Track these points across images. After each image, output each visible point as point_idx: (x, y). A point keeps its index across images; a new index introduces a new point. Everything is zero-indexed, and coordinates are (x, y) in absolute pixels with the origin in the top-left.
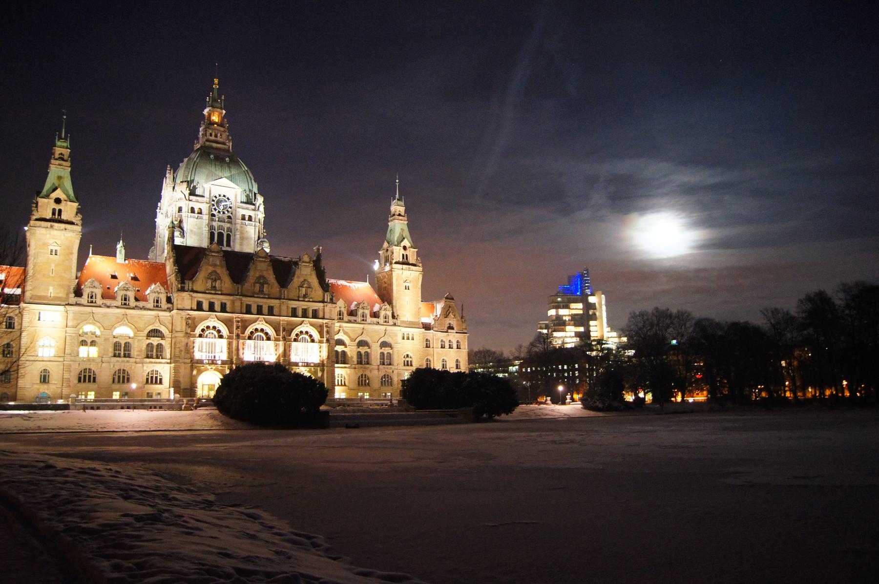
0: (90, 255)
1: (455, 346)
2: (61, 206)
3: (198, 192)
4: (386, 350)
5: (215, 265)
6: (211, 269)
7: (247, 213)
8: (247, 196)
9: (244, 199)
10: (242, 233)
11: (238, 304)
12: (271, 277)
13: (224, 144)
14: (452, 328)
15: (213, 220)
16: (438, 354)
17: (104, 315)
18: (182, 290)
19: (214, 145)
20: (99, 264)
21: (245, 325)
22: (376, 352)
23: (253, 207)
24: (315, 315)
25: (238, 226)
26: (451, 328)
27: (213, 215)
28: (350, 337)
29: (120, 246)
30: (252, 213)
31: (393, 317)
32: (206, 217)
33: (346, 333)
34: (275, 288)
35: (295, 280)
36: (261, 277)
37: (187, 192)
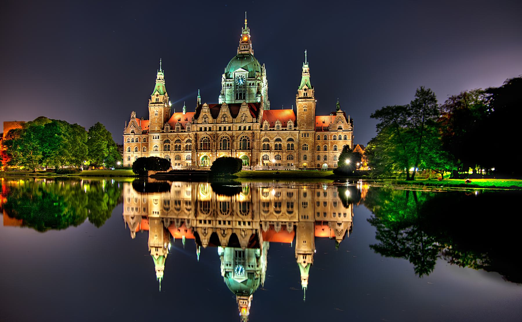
1: (343, 138)
2: (159, 97)
3: (231, 77)
6: (204, 114)
10: (249, 91)
11: (215, 127)
14: (342, 129)
15: (237, 88)
16: (331, 143)
18: (194, 123)
19: (243, 52)
22: (284, 144)
27: (237, 86)
29: (184, 109)
32: (233, 87)
34: (231, 119)
35: (239, 114)
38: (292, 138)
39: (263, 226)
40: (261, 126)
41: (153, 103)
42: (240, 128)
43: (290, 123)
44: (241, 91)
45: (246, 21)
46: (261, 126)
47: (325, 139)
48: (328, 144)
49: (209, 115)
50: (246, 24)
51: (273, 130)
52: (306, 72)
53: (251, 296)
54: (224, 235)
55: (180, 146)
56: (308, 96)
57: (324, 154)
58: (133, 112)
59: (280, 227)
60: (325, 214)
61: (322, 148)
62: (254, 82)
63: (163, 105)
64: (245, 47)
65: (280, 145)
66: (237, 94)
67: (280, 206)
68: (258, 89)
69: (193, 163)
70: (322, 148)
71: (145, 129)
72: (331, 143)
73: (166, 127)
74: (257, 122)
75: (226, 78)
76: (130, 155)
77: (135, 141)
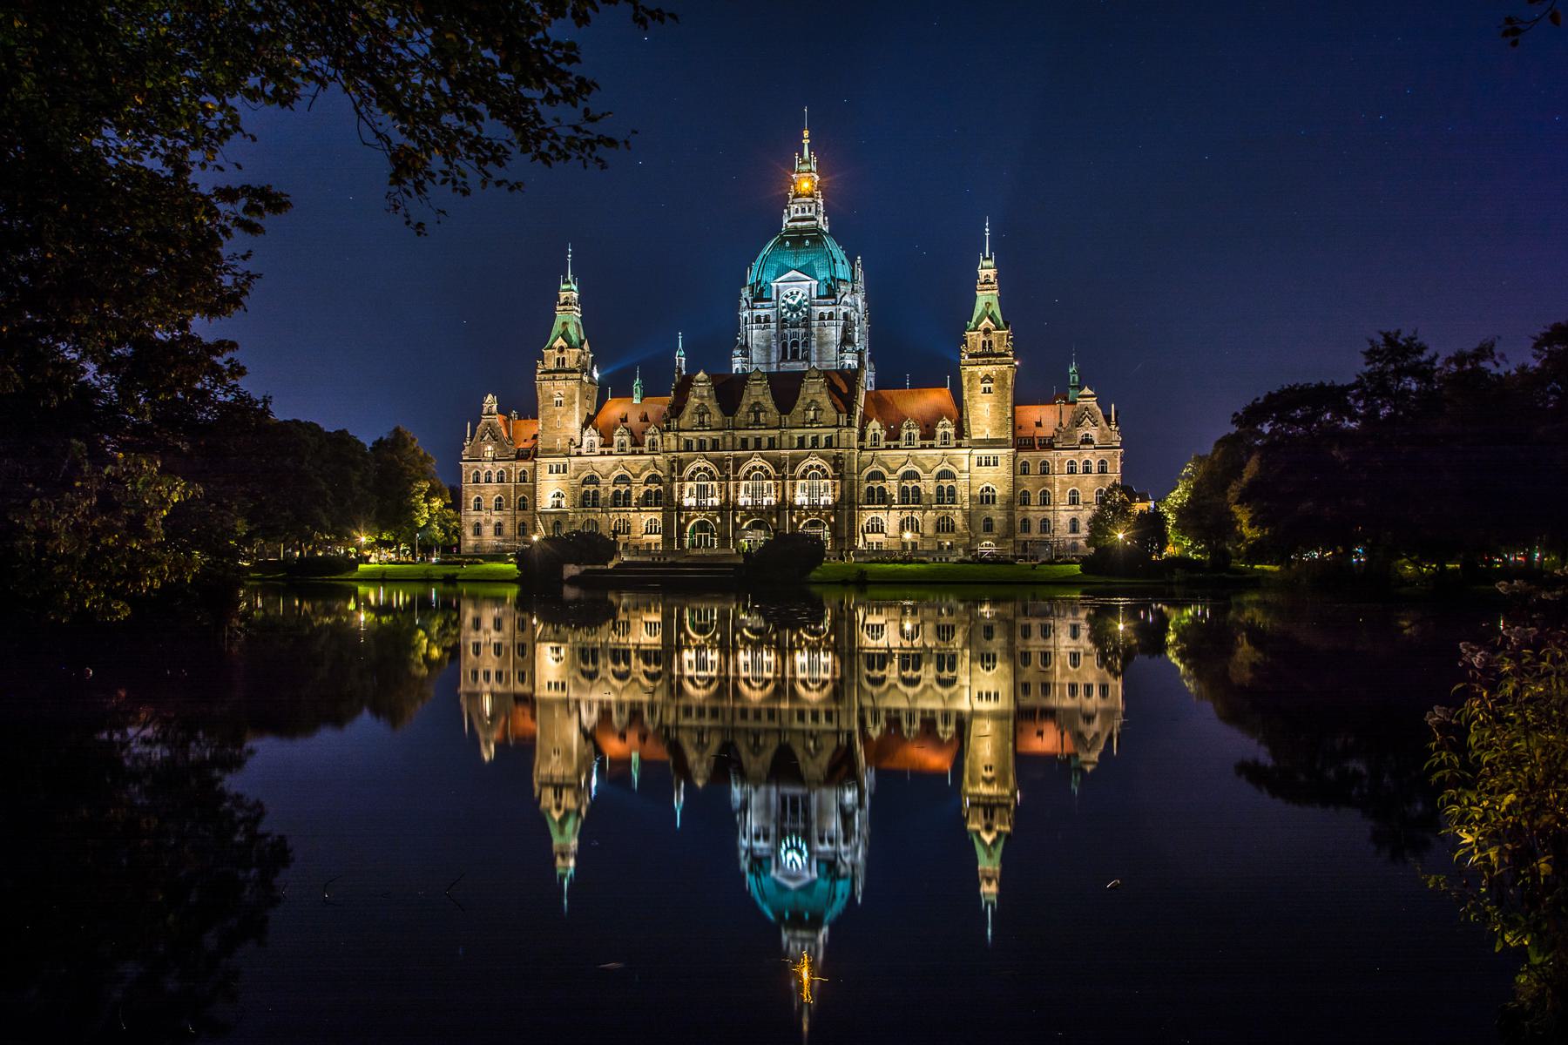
1: (1095, 468)
4: (946, 483)
5: (702, 397)
7: (826, 310)
8: (829, 287)
9: (823, 292)
10: (820, 338)
11: (729, 439)
12: (769, 403)
13: (813, 219)
16: (1062, 482)
17: (602, 464)
18: (668, 429)
20: (615, 409)
21: (738, 463)
22: (928, 486)
25: (815, 330)
26: (1087, 441)
27: (785, 320)
32: (773, 325)
34: (772, 415)
35: (799, 402)
36: (757, 403)
38: (951, 468)
39: (870, 724)
40: (862, 437)
41: (550, 372)
42: (802, 441)
44: (795, 335)
45: (806, 134)
46: (862, 437)
47: (1045, 472)
48: (1052, 485)
49: (712, 405)
50: (806, 142)
51: (896, 448)
52: (986, 282)
53: (825, 930)
54: (756, 749)
55: (628, 493)
56: (996, 348)
57: (1041, 515)
58: (490, 397)
59: (917, 726)
60: (1046, 688)
61: (1035, 497)
62: (832, 309)
63: (577, 376)
64: (803, 210)
65: (917, 490)
66: (785, 345)
67: (952, 667)
68: (845, 331)
69: (667, 540)
70: (1035, 497)
71: (523, 445)
72: (1062, 482)
73: (586, 440)
74: (850, 425)
75: (755, 300)
76: (482, 521)
77: (494, 478)
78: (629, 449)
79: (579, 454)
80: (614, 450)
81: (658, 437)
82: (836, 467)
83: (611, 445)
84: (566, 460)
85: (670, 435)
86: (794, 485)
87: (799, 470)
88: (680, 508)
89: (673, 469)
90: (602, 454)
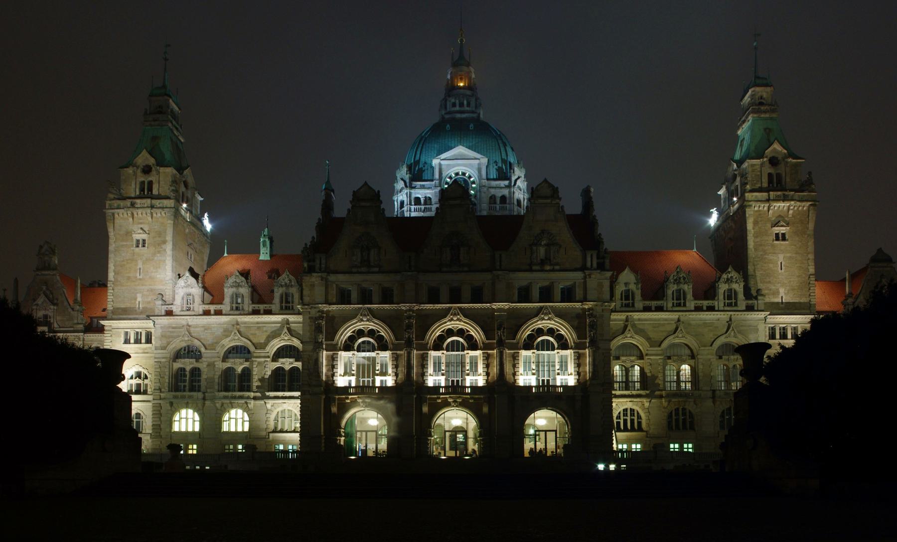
0: (226, 255)
8: (499, 170)
9: (493, 174)
23: (507, 183)
24: (568, 295)
28: (648, 339)
30: (506, 192)
31: (748, 294)
33: (640, 332)
37: (407, 177)
43: (729, 281)
75: (412, 179)
78: (248, 306)
79: (169, 313)
80: (225, 307)
81: (294, 291)
82: (579, 330)
83: (220, 302)
84: (149, 324)
85: (315, 278)
86: (515, 357)
87: (526, 332)
88: (330, 387)
89: (318, 329)
90: (207, 313)
